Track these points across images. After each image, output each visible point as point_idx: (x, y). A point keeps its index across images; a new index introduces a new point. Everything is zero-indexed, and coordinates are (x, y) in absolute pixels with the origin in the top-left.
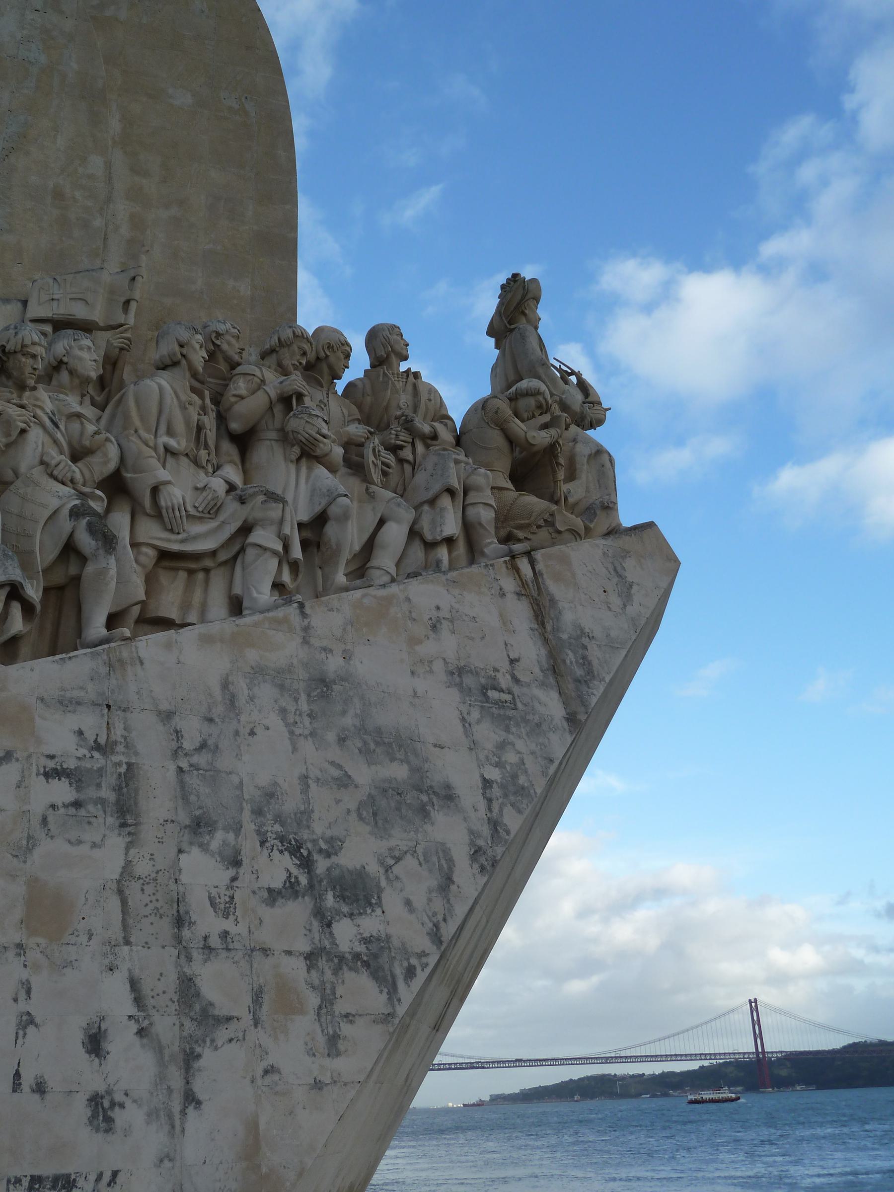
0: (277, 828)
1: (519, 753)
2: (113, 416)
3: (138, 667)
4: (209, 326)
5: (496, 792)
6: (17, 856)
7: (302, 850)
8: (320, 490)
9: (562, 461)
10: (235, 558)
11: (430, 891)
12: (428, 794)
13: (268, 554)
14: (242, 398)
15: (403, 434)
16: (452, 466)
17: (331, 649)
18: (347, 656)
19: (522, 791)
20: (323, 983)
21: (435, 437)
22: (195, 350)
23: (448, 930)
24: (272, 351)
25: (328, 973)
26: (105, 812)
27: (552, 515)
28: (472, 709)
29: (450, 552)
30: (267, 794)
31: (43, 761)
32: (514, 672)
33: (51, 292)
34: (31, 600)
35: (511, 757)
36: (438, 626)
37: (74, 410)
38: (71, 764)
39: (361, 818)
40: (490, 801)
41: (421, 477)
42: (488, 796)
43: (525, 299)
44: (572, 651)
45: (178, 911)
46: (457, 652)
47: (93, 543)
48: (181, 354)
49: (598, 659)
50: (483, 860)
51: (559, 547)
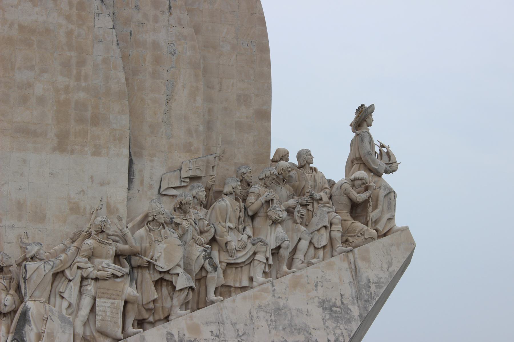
1: (341, 330)
8: (279, 237)
9: (371, 204)
10: (251, 262)
13: (262, 263)
14: (253, 203)
15: (309, 200)
16: (326, 216)
17: (281, 298)
21: (321, 199)
24: (262, 179)
29: (324, 250)
32: (342, 300)
35: (338, 331)
36: (317, 285)
37: (201, 218)
41: (314, 220)
44: (365, 289)
47: (211, 268)
49: (375, 291)
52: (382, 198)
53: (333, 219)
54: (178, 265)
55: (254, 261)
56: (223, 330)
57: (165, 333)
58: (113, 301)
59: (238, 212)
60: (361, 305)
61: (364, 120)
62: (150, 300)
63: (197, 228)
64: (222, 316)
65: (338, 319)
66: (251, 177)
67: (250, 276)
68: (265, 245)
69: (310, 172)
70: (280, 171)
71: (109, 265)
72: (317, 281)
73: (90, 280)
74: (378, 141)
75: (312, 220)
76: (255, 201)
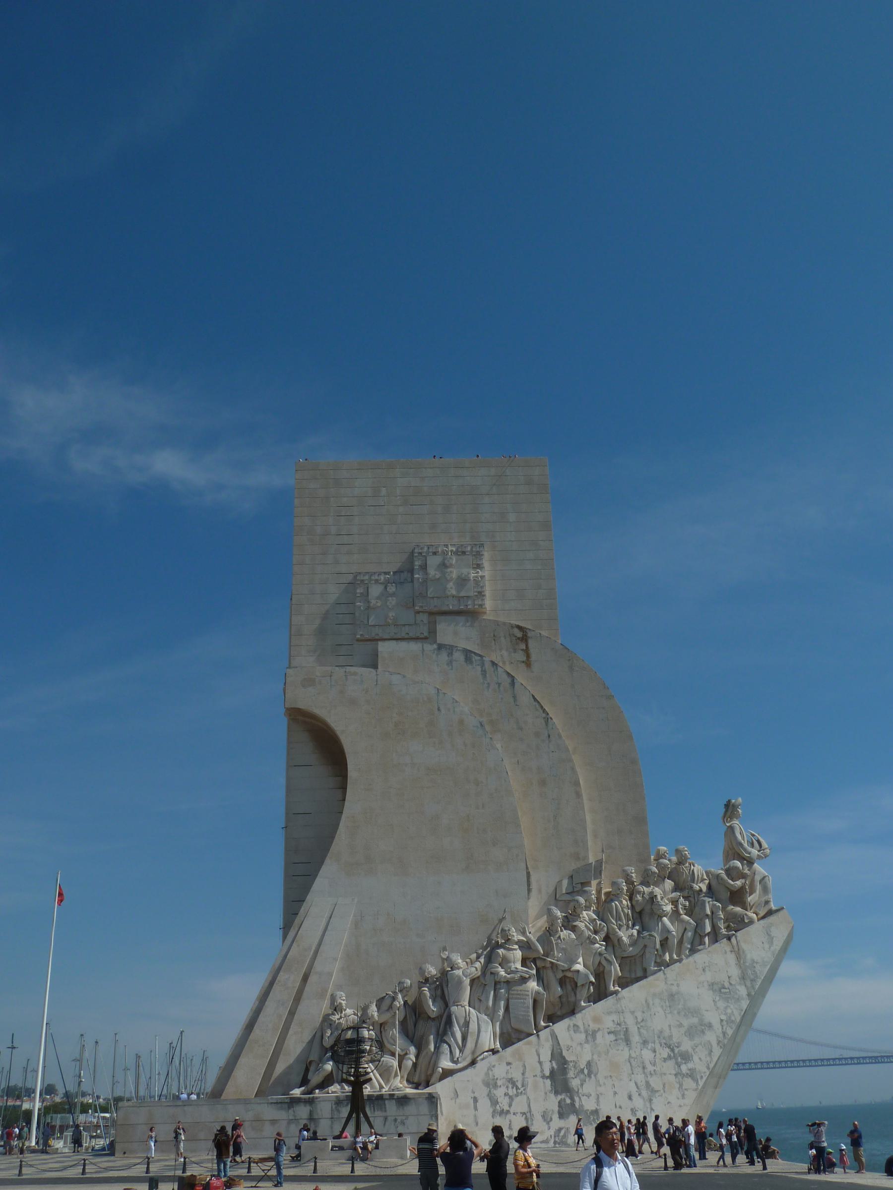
1: (731, 1009)
5: (725, 1023)
10: (643, 955)
11: (706, 1055)
18: (678, 985)
19: (733, 1022)
20: (679, 1081)
21: (701, 890)
23: (711, 1066)
25: (681, 1079)
27: (743, 917)
31: (607, 1030)
35: (729, 1011)
38: (613, 1030)
39: (685, 1035)
40: (722, 1026)
50: (721, 1045)
56: (624, 1018)
57: (572, 1025)
63: (592, 928)
64: (621, 1006)
67: (644, 967)
71: (516, 968)
73: (502, 984)
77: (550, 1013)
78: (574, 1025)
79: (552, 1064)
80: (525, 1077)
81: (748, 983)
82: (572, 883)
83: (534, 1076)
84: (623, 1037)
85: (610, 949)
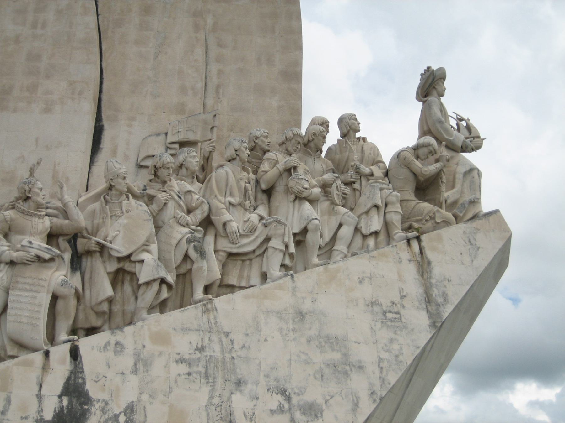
0: (275, 383)
2: (206, 188)
3: (215, 312)
4: (252, 133)
6: (165, 395)
7: (286, 393)
9: (444, 180)
12: (350, 366)
13: (278, 251)
14: (266, 172)
16: (378, 192)
18: (314, 301)
21: (372, 175)
22: (243, 152)
24: (283, 143)
26: (200, 377)
28: (377, 322)
29: (376, 238)
30: (271, 368)
32: (403, 303)
33: (178, 128)
34: (170, 283)
36: (363, 281)
37: (187, 189)
38: (186, 357)
39: (315, 378)
41: (363, 199)
42: (381, 366)
43: (435, 80)
44: (437, 288)
45: (230, 419)
46: (372, 294)
47: (196, 255)
48: (236, 154)
50: (375, 397)
51: (437, 231)
52: (461, 176)
53: (387, 197)
54: (148, 251)
55: (268, 249)
57: (113, 343)
58: (32, 294)
59: (243, 184)
60: (431, 311)
61: (433, 86)
62: (100, 299)
63: (182, 203)
65: (395, 329)
66: (269, 143)
68: (282, 225)
69: (356, 141)
70: (310, 137)
71: (30, 242)
72: (363, 277)
74: (453, 112)
75: (359, 201)
76: (270, 169)
77: (87, 326)
78: (117, 344)
79: (61, 402)
80: (6, 418)
81: (432, 308)
82: (166, 143)
83: (22, 418)
84: (201, 369)
85: (210, 239)
